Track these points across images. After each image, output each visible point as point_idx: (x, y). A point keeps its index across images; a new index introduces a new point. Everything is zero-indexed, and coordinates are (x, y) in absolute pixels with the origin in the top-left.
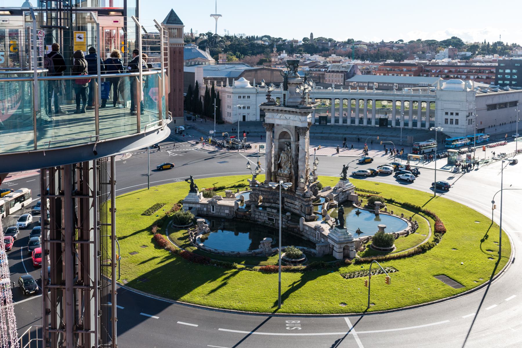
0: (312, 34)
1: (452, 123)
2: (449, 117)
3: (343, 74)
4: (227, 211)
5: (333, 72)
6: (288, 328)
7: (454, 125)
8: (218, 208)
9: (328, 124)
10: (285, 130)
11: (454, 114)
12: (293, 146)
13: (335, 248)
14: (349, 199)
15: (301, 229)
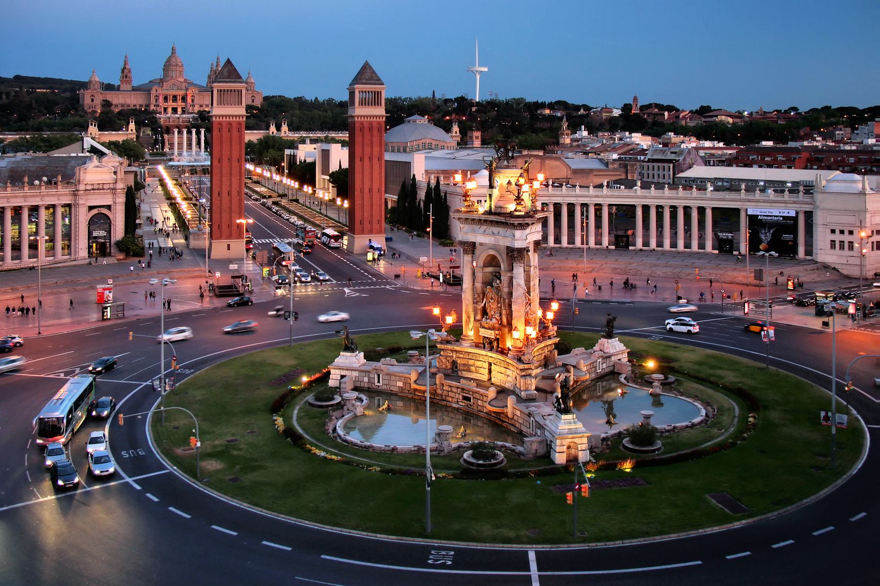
0: (635, 99)
1: (842, 247)
2: (837, 237)
3: (671, 165)
4: (400, 384)
5: (654, 161)
6: (430, 562)
7: (846, 252)
8: (387, 377)
10: (492, 252)
11: (846, 232)
12: (504, 278)
14: (616, 370)
15: (510, 415)
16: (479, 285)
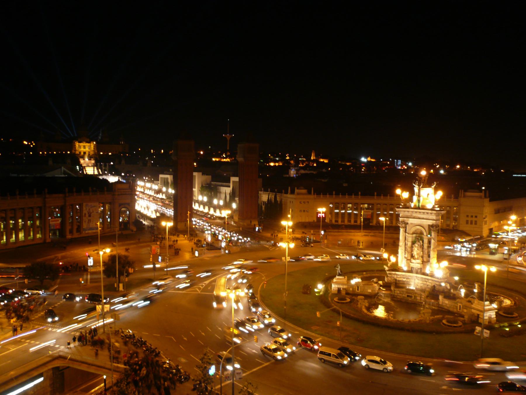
2: (470, 219)
7: (473, 225)
9: (371, 224)
13: (480, 316)
15: (440, 303)
16: (409, 244)
